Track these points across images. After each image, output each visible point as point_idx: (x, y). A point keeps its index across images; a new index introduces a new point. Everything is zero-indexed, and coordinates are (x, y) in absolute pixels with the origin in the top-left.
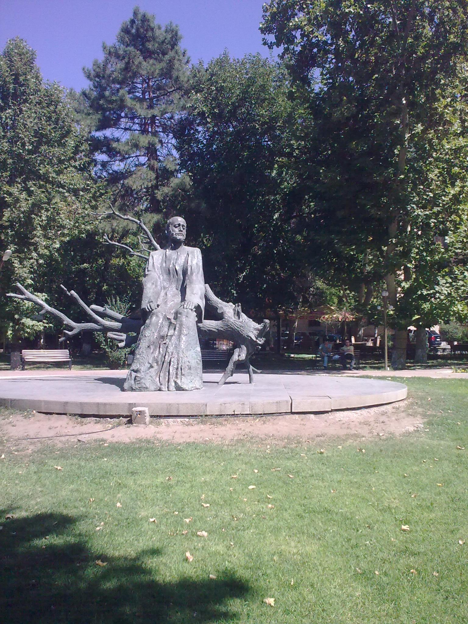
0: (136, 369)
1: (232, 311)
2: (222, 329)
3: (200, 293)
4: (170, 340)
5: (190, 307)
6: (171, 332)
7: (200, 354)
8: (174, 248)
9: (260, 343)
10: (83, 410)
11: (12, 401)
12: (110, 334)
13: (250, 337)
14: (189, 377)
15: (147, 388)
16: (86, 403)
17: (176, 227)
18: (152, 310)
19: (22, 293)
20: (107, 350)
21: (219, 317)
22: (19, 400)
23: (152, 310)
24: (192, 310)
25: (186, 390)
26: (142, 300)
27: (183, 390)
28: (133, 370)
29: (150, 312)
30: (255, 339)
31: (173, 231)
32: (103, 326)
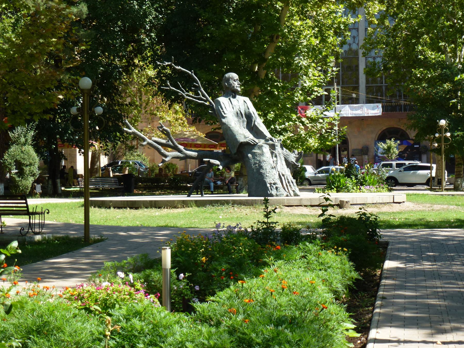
0: (273, 182)
4: (277, 164)
6: (275, 159)
8: (234, 97)
10: (311, 203)
16: (313, 199)
17: (235, 81)
18: (257, 143)
19: (130, 129)
20: (17, 179)
23: (257, 143)
26: (235, 136)
31: (234, 84)
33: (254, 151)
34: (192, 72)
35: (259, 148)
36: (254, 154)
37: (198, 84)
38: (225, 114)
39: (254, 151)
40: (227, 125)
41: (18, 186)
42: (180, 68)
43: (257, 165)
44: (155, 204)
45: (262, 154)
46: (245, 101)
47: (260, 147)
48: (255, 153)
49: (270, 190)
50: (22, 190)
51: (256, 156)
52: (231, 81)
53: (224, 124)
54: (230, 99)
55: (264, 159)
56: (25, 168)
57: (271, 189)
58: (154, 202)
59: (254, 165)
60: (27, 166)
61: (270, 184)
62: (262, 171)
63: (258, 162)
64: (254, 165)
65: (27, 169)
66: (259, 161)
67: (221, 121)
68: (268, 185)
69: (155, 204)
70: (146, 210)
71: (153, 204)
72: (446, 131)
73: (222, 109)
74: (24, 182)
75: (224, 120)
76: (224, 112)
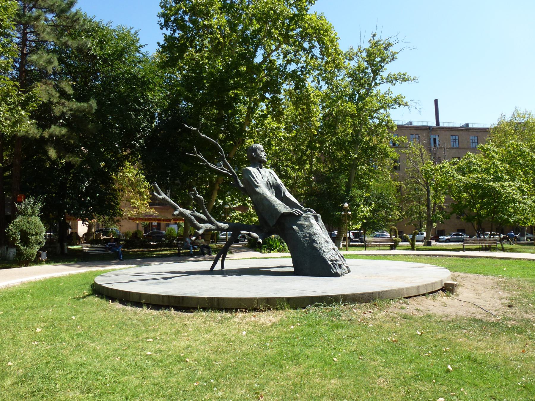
11: (379, 293)
20: (22, 248)
22: (386, 291)
26: (274, 206)
32: (217, 226)
33: (299, 222)
34: (217, 141)
35: (305, 219)
36: (301, 227)
37: (222, 153)
38: (258, 183)
39: (299, 222)
40: (263, 195)
41: (23, 254)
42: (204, 135)
43: (308, 238)
44: (218, 304)
45: (311, 226)
46: (270, 173)
47: (307, 219)
48: (301, 224)
49: (333, 268)
50: (27, 258)
51: (304, 228)
52: (259, 152)
53: (259, 193)
54: (258, 169)
55: (315, 231)
56: (30, 237)
57: (335, 268)
58: (216, 300)
59: (303, 238)
60: (33, 235)
61: (331, 261)
62: (315, 245)
63: (308, 235)
64: (303, 238)
65: (32, 239)
66: (309, 234)
67: (255, 190)
68: (330, 263)
69: (218, 304)
70: (204, 314)
71: (215, 304)
72: (348, 211)
73: (254, 178)
74: (29, 250)
75: (257, 189)
76: (256, 181)
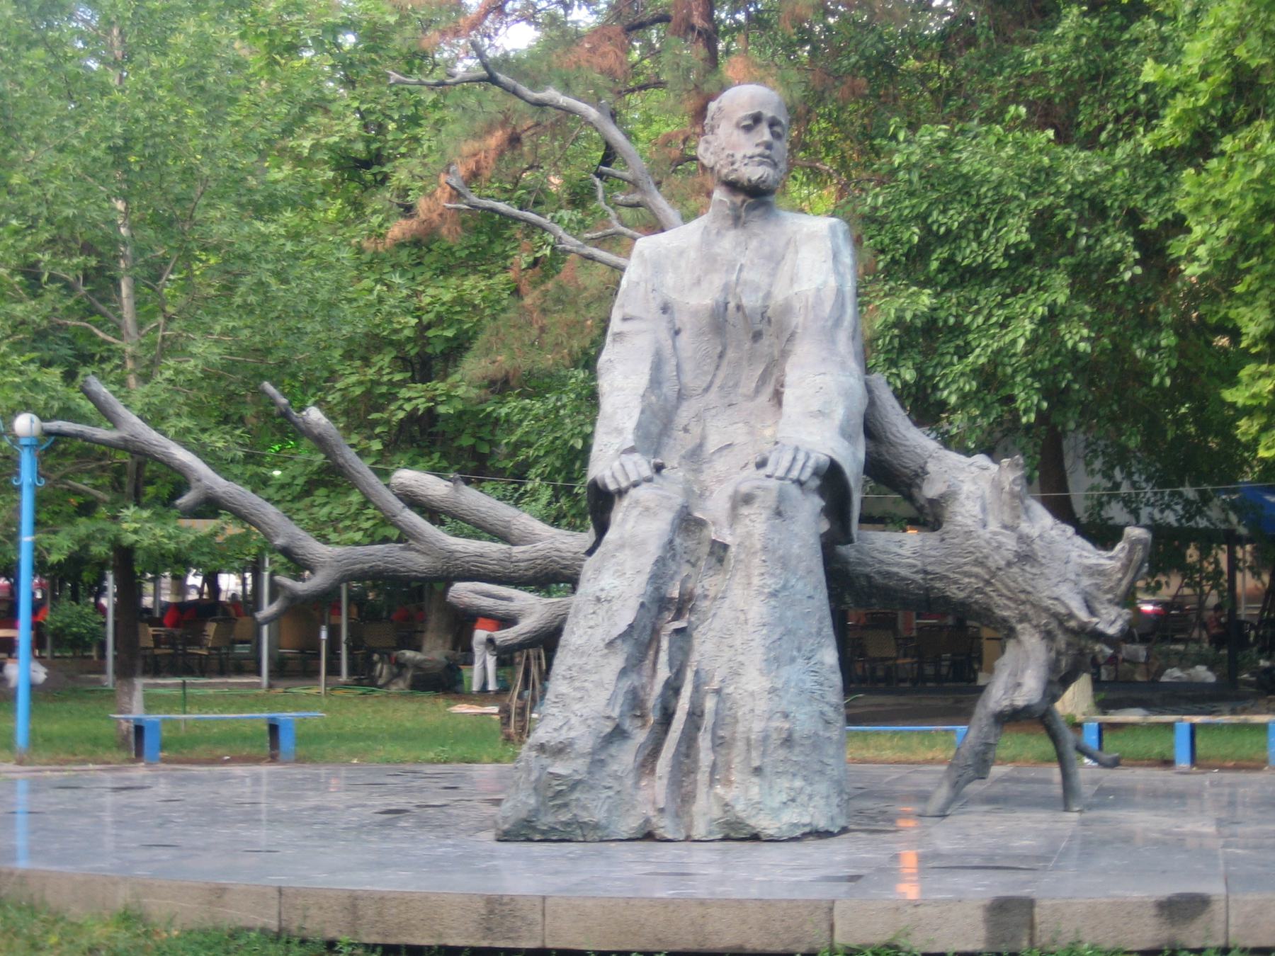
1: (986, 487)
2: (938, 569)
3: (839, 413)
5: (795, 474)
7: (837, 679)
9: (1112, 631)
12: (464, 592)
13: (1063, 603)
14: (784, 783)
15: (596, 827)
21: (929, 517)
24: (800, 483)
25: (772, 840)
27: (755, 838)
28: (542, 748)
29: (621, 493)
30: (1083, 615)
